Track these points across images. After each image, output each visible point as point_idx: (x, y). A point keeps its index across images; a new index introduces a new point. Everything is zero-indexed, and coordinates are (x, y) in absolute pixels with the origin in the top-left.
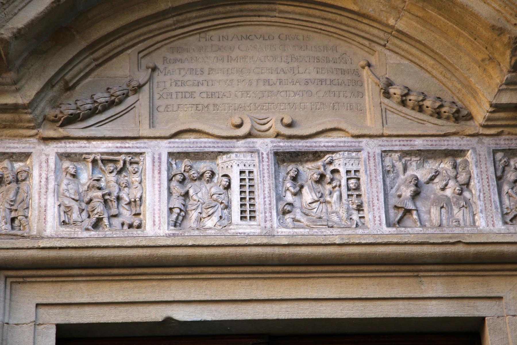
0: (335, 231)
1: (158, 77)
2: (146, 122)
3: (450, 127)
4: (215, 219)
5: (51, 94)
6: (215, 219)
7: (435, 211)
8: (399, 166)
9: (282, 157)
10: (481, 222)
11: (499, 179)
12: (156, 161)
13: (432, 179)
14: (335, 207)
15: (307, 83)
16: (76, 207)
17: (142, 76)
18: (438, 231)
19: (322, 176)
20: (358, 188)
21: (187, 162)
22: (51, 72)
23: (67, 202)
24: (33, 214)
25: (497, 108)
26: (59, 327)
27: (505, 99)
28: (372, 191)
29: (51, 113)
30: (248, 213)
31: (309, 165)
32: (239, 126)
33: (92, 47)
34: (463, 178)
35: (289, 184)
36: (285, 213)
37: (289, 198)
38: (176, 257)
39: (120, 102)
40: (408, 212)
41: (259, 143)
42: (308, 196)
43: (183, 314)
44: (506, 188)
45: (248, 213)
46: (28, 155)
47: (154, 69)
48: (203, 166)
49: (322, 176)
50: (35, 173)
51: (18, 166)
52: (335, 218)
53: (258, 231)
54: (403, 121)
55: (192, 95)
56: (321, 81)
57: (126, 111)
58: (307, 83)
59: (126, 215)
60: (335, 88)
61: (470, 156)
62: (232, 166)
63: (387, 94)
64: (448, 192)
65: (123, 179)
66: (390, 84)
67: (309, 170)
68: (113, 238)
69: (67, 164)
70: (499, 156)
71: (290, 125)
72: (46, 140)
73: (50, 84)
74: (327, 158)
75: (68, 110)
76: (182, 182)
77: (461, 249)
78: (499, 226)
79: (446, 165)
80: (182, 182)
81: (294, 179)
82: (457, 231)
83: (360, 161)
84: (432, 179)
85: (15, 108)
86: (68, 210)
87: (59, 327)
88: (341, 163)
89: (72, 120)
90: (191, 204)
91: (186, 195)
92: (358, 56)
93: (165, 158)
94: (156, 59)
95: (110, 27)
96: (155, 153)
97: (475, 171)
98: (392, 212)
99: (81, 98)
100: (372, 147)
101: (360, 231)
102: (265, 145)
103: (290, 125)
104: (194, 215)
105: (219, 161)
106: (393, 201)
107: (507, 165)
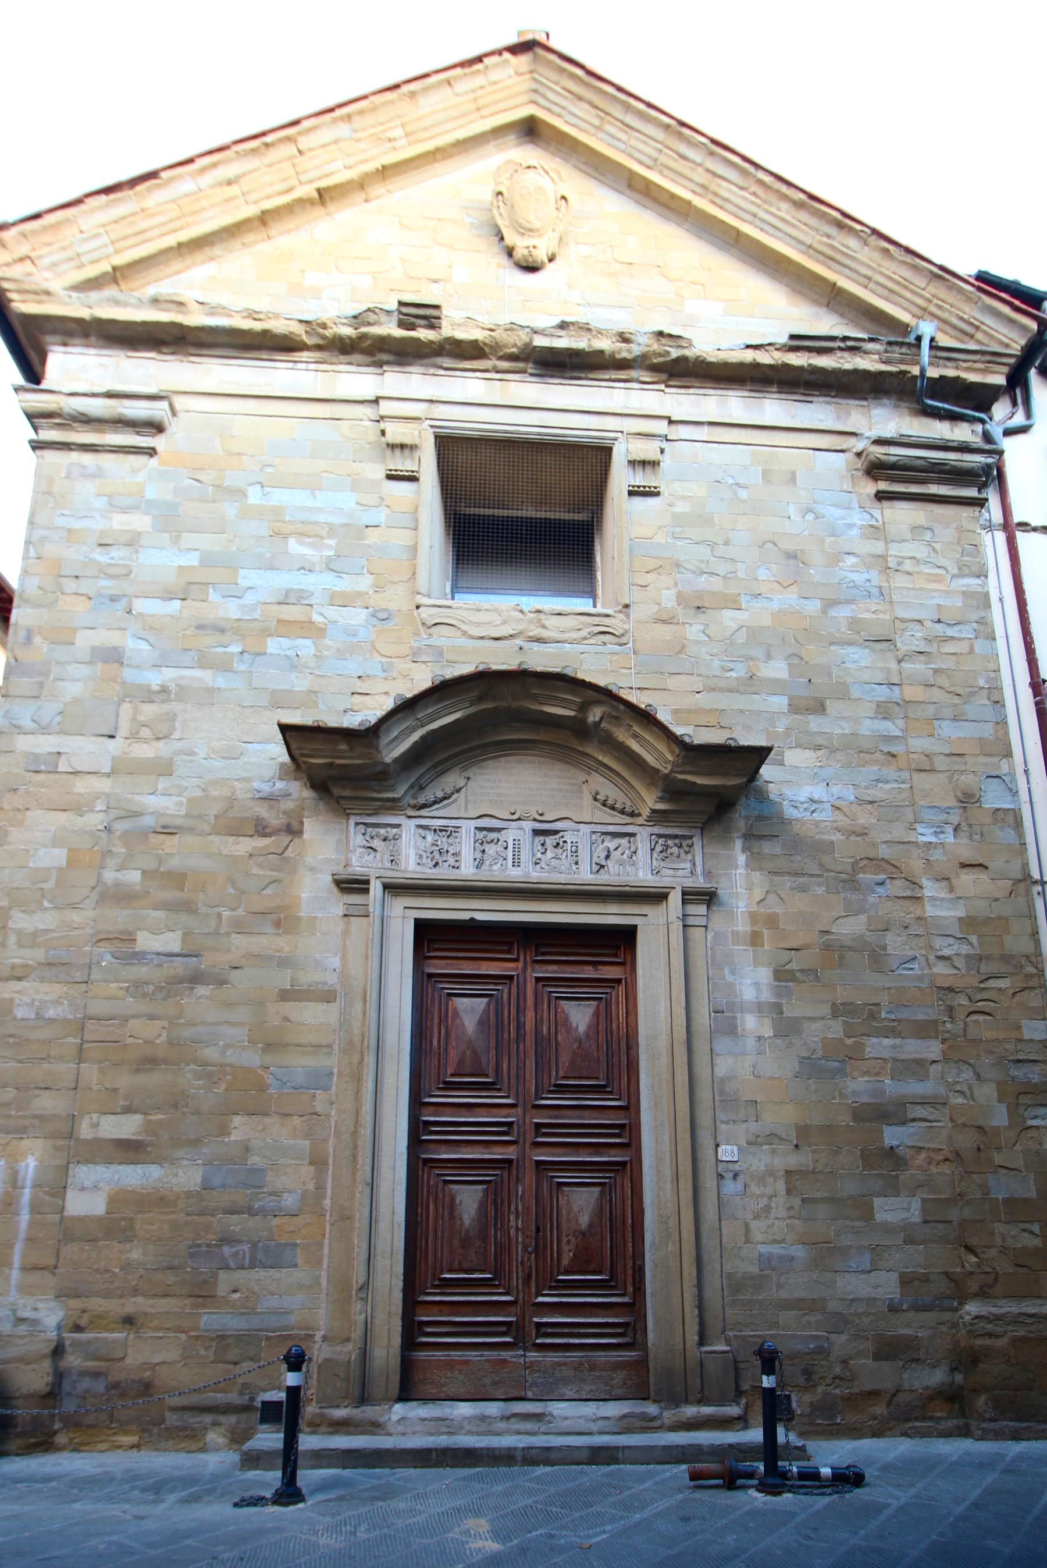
0: (563, 876)
1: (470, 783)
2: (463, 808)
3: (629, 820)
4: (499, 865)
5: (412, 792)
6: (499, 865)
7: (617, 867)
8: (600, 840)
9: (537, 833)
10: (641, 874)
11: (652, 850)
12: (468, 832)
13: (617, 848)
14: (564, 862)
15: (552, 790)
16: (424, 855)
17: (461, 782)
18: (617, 878)
19: (558, 844)
20: (576, 852)
21: (485, 833)
22: (412, 780)
23: (421, 853)
24: (403, 858)
25: (654, 811)
26: (416, 919)
27: (660, 806)
28: (584, 855)
29: (412, 802)
30: (516, 864)
31: (552, 837)
32: (513, 814)
33: (434, 766)
34: (633, 849)
35: (540, 848)
36: (536, 864)
37: (539, 855)
38: (477, 887)
39: (449, 797)
40: (602, 867)
41: (523, 824)
42: (550, 854)
43: (480, 917)
44: (655, 855)
45: (516, 864)
46: (398, 826)
47: (468, 779)
48: (493, 835)
49: (558, 844)
50: (404, 836)
51: (395, 830)
52: (563, 868)
53: (521, 873)
54: (604, 815)
55: (489, 794)
56: (560, 790)
57: (453, 802)
58: (552, 790)
59: (451, 861)
60: (568, 794)
61: (638, 837)
62: (510, 835)
63: (596, 799)
64: (625, 856)
65: (451, 840)
66: (597, 794)
67: (550, 841)
68: (444, 874)
69: (420, 831)
70: (653, 837)
71: (541, 815)
72: (410, 817)
73: (412, 787)
74: (561, 834)
75: (422, 800)
76: (482, 843)
77: (628, 889)
78: (650, 877)
79: (624, 841)
80: (482, 843)
81: (543, 845)
82: (627, 878)
83: (579, 836)
84: (617, 848)
85: (394, 800)
86: (421, 857)
87: (416, 919)
88: (569, 837)
89: (424, 806)
90: (486, 857)
91: (484, 851)
92: (583, 777)
93: (473, 830)
94: (469, 773)
95: (445, 755)
96: (468, 827)
97: (640, 846)
98: (594, 866)
99: (428, 795)
100: (585, 829)
101: (576, 876)
102: (528, 826)
103: (541, 815)
104: (487, 862)
105: (503, 832)
106: (595, 859)
107: (657, 842)
